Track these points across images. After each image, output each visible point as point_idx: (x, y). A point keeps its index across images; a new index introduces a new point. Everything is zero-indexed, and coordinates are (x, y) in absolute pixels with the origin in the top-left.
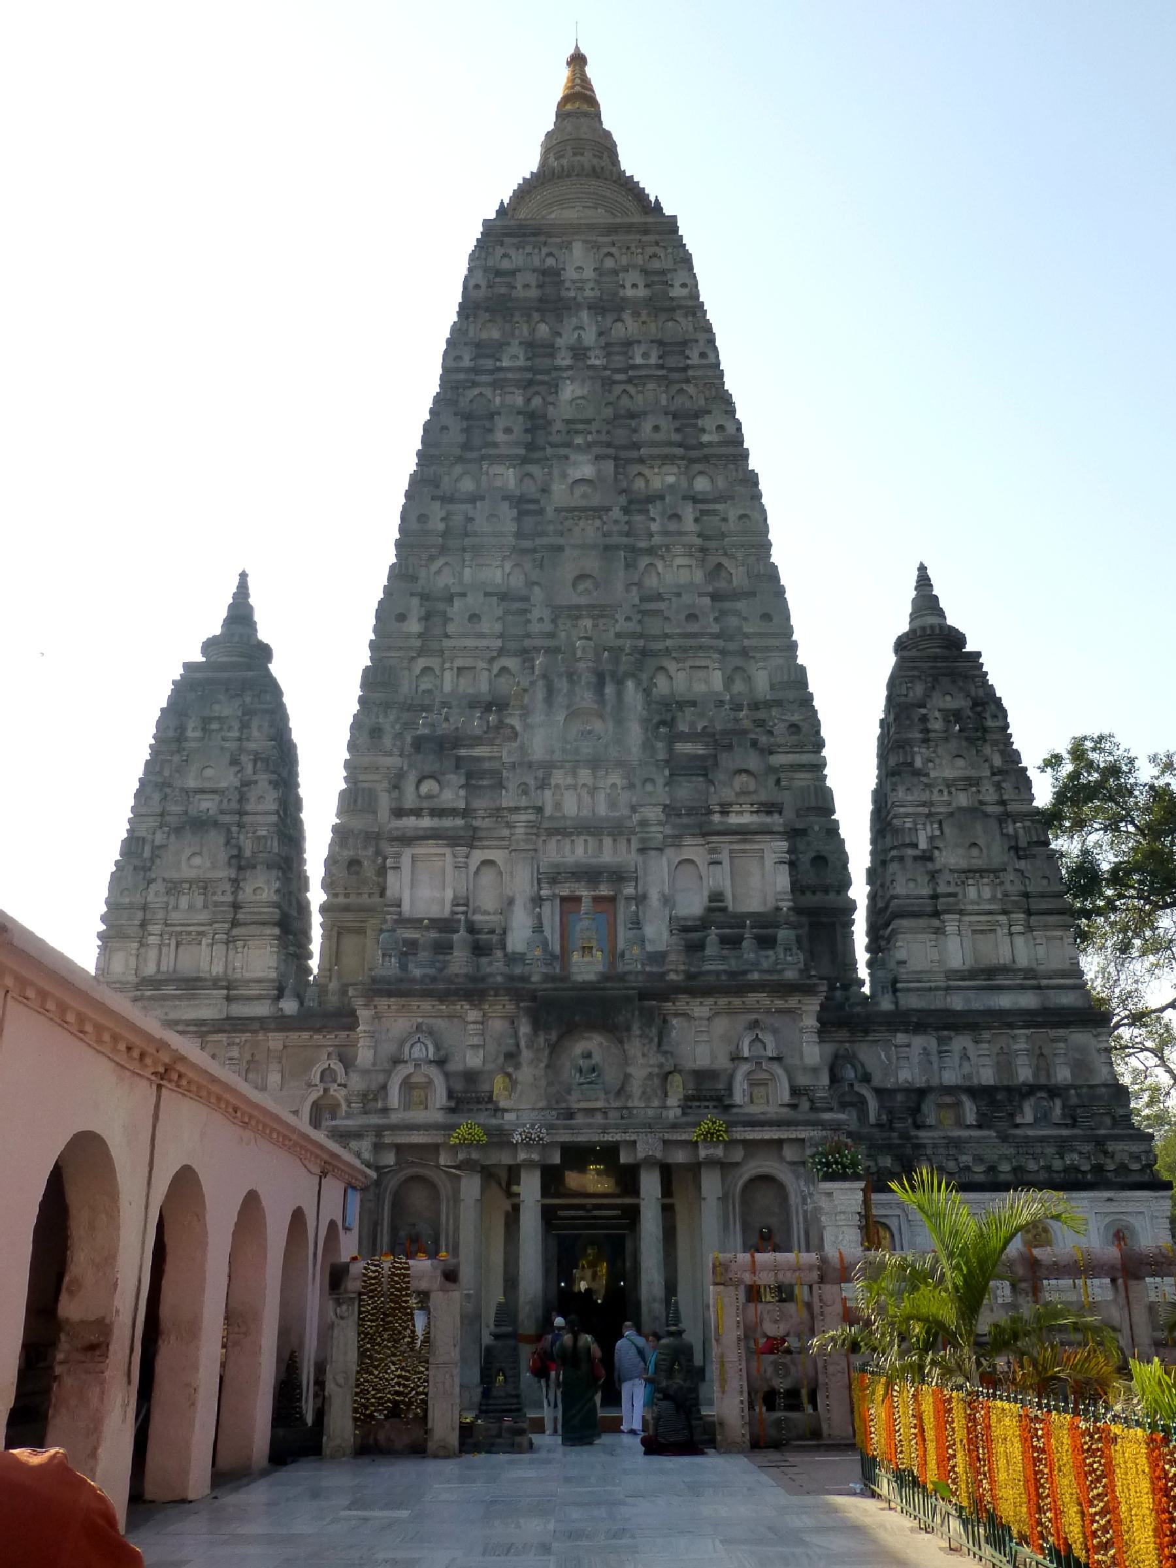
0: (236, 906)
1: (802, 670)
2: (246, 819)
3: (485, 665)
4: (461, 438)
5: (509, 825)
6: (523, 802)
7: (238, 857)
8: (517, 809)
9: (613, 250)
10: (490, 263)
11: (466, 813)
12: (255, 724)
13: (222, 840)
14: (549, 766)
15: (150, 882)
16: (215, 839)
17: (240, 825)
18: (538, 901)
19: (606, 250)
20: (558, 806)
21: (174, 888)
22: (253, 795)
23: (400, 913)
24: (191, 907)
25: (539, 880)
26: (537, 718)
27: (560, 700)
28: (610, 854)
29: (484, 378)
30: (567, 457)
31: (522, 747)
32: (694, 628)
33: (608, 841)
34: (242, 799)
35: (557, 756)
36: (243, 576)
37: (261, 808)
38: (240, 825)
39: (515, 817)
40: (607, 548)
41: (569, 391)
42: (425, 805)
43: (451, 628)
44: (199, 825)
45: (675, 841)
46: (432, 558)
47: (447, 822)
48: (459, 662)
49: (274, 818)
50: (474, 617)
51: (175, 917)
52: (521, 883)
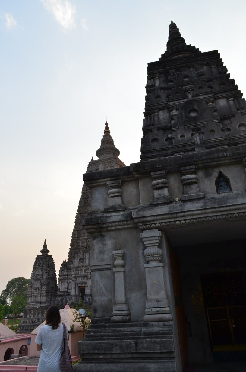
0: (41, 291)
2: (43, 278)
3: (85, 241)
4: (84, 203)
6: (73, 273)
7: (42, 284)
8: (73, 274)
9: (107, 163)
10: (89, 170)
11: (67, 275)
12: (44, 264)
13: (39, 282)
14: (77, 267)
16: (39, 281)
17: (42, 279)
18: (75, 288)
19: (105, 164)
20: (78, 273)
21: (35, 289)
23: (60, 290)
24: (37, 291)
25: (75, 285)
26: (76, 260)
27: (79, 257)
28: (84, 280)
31: (74, 265)
33: (84, 278)
34: (42, 275)
35: (78, 266)
36: (45, 240)
37: (44, 276)
38: (42, 279)
39: (73, 276)
42: (62, 274)
43: (81, 235)
44: (37, 279)
46: (80, 224)
47: (65, 277)
48: (82, 241)
50: (84, 233)
51: (35, 293)
52: (73, 285)
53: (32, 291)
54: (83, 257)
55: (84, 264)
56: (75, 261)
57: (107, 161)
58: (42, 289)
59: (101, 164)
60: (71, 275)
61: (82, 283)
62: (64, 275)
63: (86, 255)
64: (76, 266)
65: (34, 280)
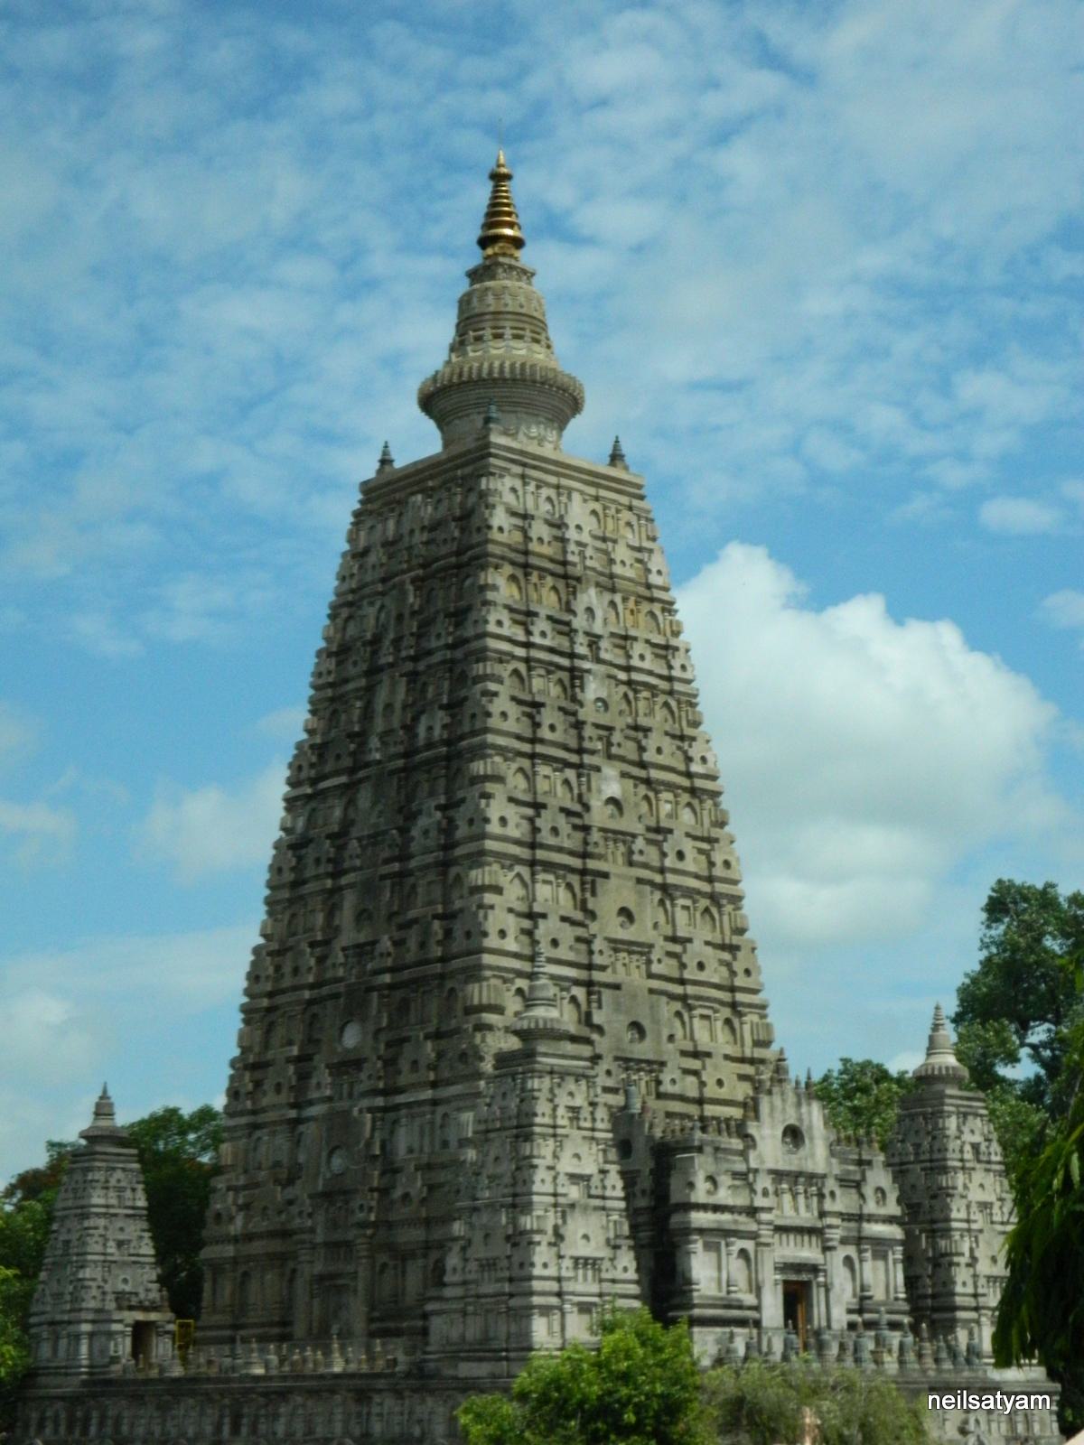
1: (768, 1027)
5: (759, 1223)
9: (597, 506)
15: (560, 1257)
22: (608, 1183)
26: (766, 1131)
27: (778, 1115)
28: (807, 1252)
29: (521, 652)
30: (598, 769)
32: (702, 976)
39: (764, 1216)
40: (640, 881)
41: (593, 689)
45: (844, 1241)
49: (622, 1205)
53: (564, 1273)
54: (800, 1119)
55: (810, 1167)
56: (762, 1138)
57: (603, 493)
58: (619, 1275)
59: (576, 496)
60: (752, 1211)
61: (798, 1267)
62: (717, 1208)
63: (810, 1113)
64: (771, 1165)
65: (555, 1205)
